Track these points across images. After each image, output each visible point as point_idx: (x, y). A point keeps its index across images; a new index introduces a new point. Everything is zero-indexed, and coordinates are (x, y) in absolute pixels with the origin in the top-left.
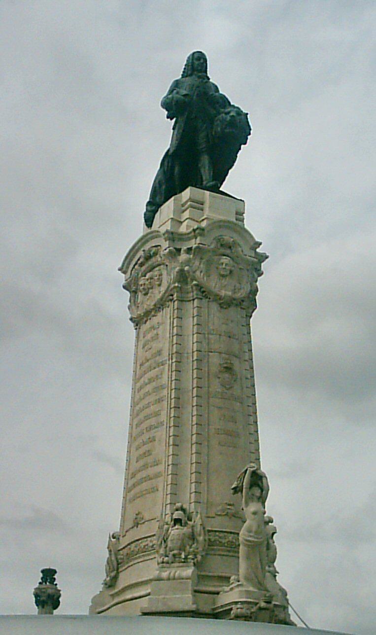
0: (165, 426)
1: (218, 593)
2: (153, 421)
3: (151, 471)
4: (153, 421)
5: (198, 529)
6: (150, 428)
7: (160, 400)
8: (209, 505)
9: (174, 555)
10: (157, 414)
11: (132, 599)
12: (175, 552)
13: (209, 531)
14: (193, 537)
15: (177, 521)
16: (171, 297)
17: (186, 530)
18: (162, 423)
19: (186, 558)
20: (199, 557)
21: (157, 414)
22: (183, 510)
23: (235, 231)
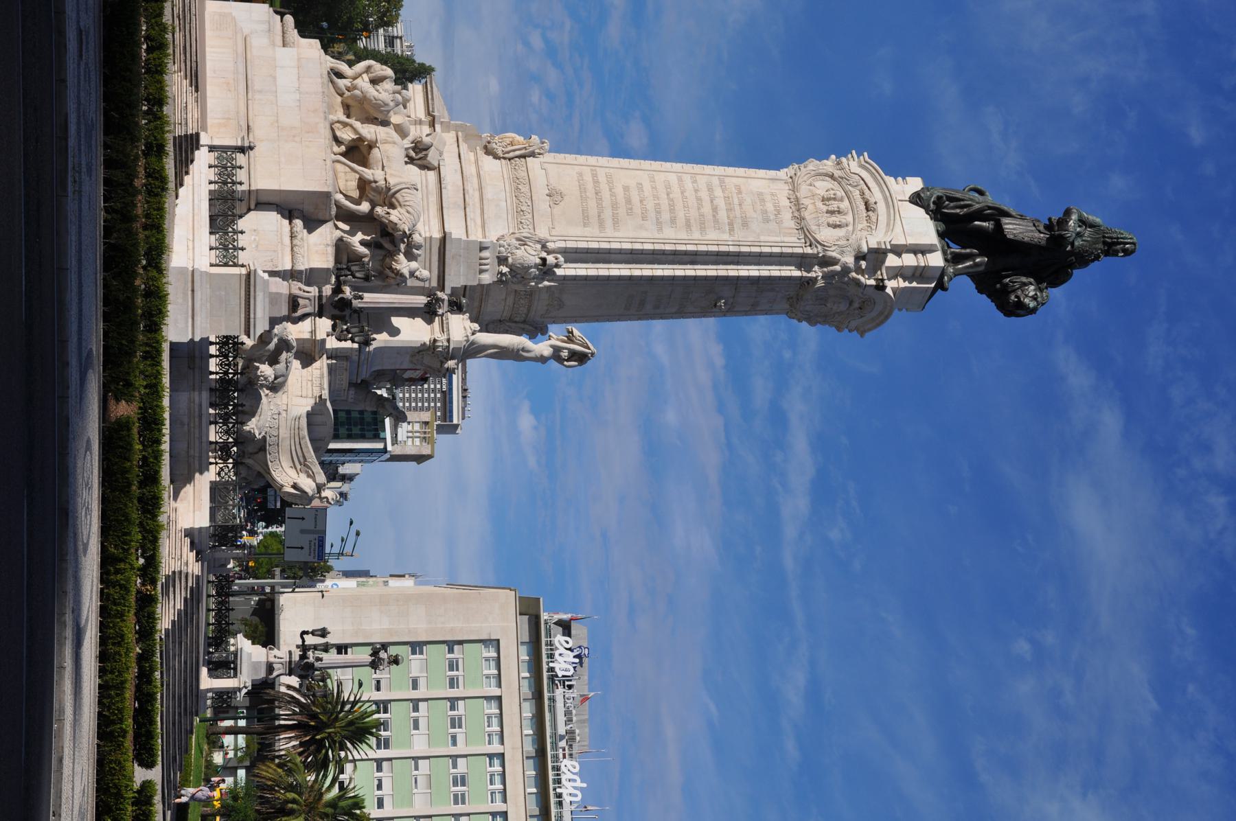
0: (657, 236)
3: (608, 214)
4: (666, 216)
6: (658, 212)
18: (660, 229)
21: (673, 221)
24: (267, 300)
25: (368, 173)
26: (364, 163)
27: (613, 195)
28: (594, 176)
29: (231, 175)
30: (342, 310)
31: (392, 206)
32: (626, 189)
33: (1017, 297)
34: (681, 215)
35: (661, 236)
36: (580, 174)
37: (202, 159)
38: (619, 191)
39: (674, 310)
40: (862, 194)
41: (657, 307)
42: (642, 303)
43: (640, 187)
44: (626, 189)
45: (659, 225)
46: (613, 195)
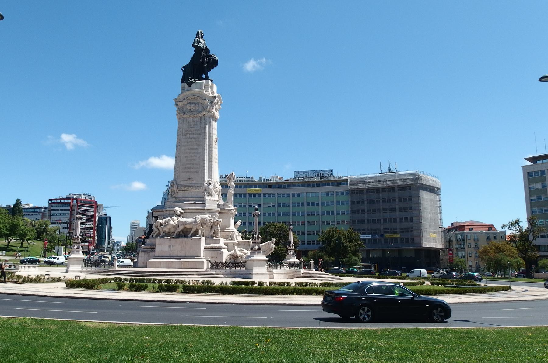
4: (195, 151)
6: (194, 153)
32: (187, 160)
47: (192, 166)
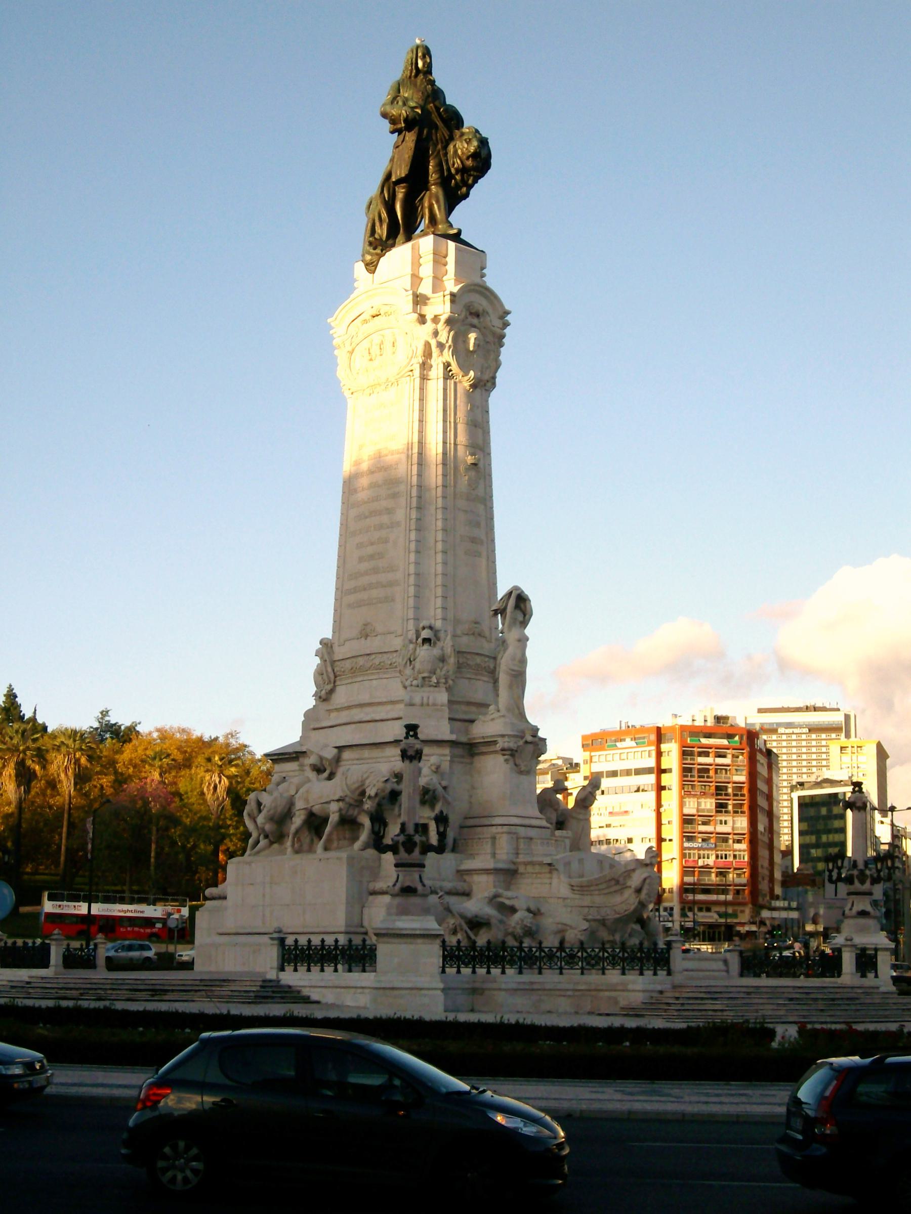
0: (403, 526)
1: (472, 721)
2: (385, 519)
3: (383, 578)
4: (385, 519)
5: (449, 650)
6: (380, 527)
7: (395, 496)
8: (457, 622)
9: (424, 678)
10: (389, 511)
11: (360, 722)
12: (426, 675)
13: (459, 652)
14: (443, 659)
15: (426, 641)
16: (410, 373)
17: (436, 651)
18: (398, 524)
19: (438, 683)
20: (450, 682)
21: (389, 511)
22: (431, 628)
23: (486, 297)
24: (404, 917)
25: (334, 818)
26: (325, 820)
27: (366, 573)
28: (355, 590)
29: (329, 952)
30: (415, 844)
31: (363, 793)
32: (361, 560)
33: (468, 159)
34: (384, 504)
35: (403, 523)
36: (350, 606)
37: (292, 978)
38: (364, 566)
39: (483, 507)
40: (365, 321)
41: (478, 525)
42: (473, 540)
43: (360, 546)
44: (361, 560)
45: (393, 525)
46: (366, 573)
47: (373, 579)
